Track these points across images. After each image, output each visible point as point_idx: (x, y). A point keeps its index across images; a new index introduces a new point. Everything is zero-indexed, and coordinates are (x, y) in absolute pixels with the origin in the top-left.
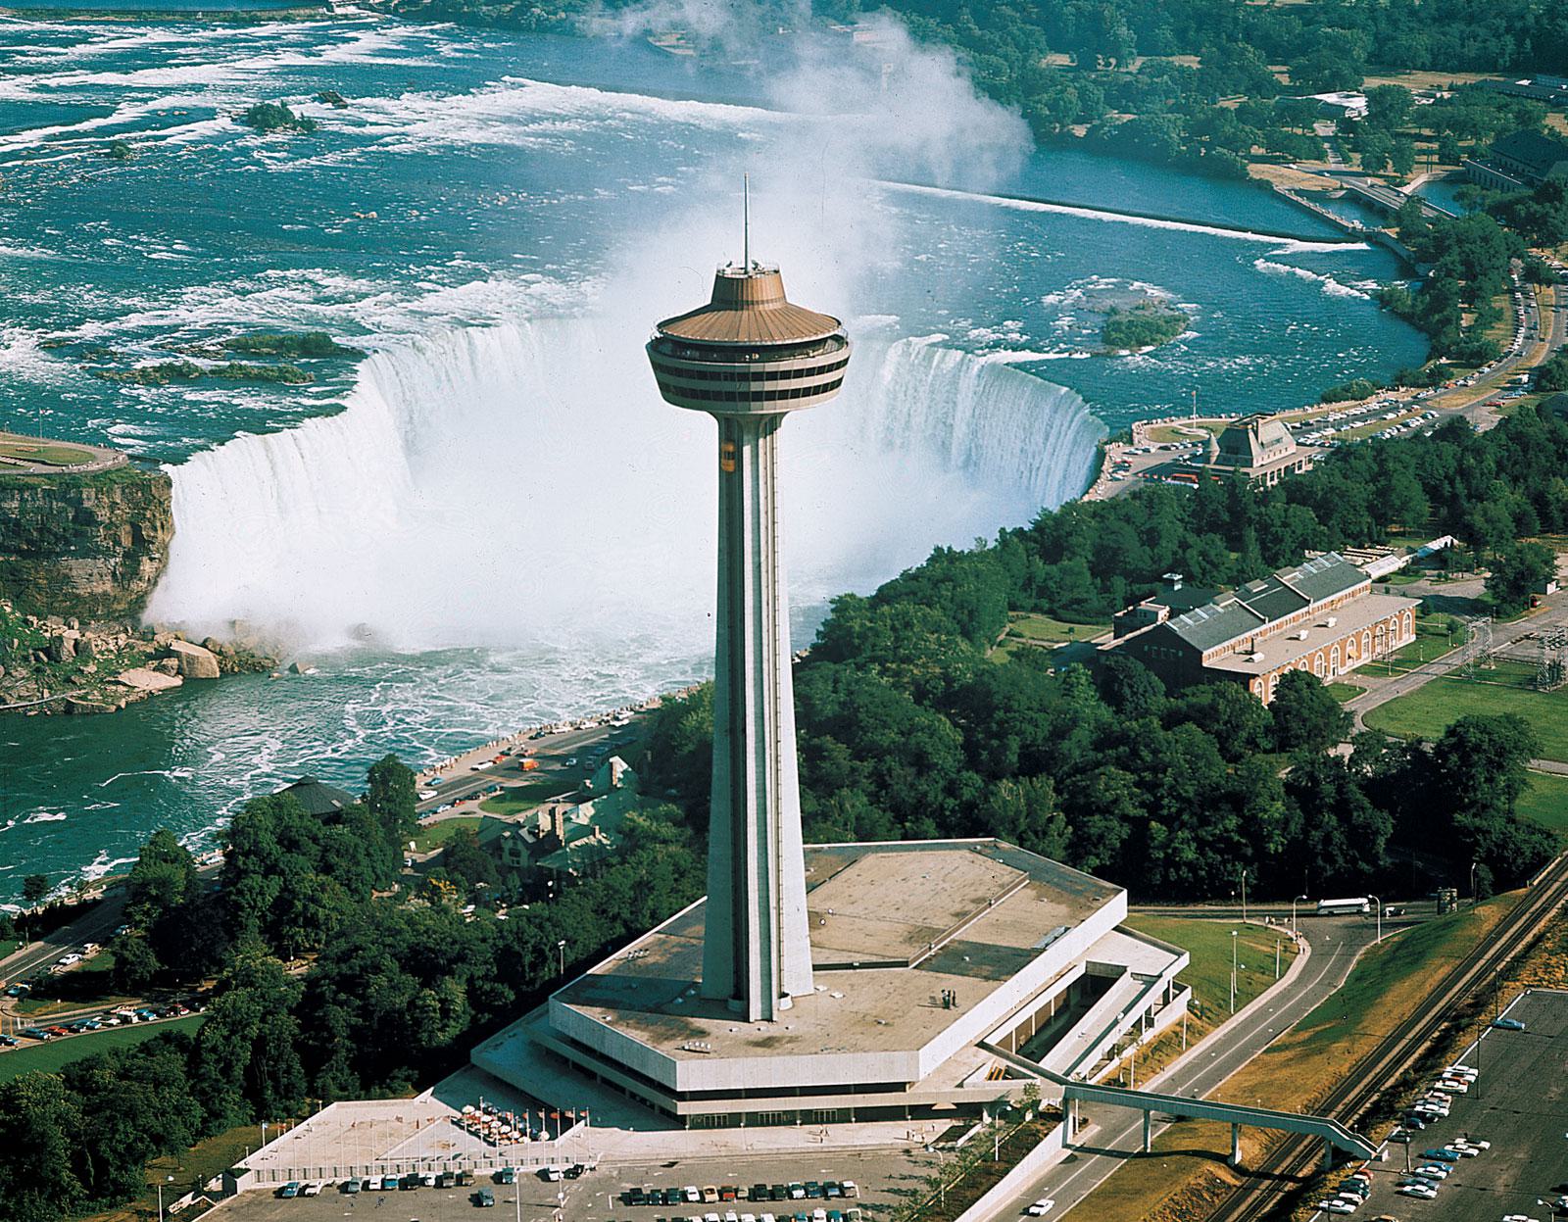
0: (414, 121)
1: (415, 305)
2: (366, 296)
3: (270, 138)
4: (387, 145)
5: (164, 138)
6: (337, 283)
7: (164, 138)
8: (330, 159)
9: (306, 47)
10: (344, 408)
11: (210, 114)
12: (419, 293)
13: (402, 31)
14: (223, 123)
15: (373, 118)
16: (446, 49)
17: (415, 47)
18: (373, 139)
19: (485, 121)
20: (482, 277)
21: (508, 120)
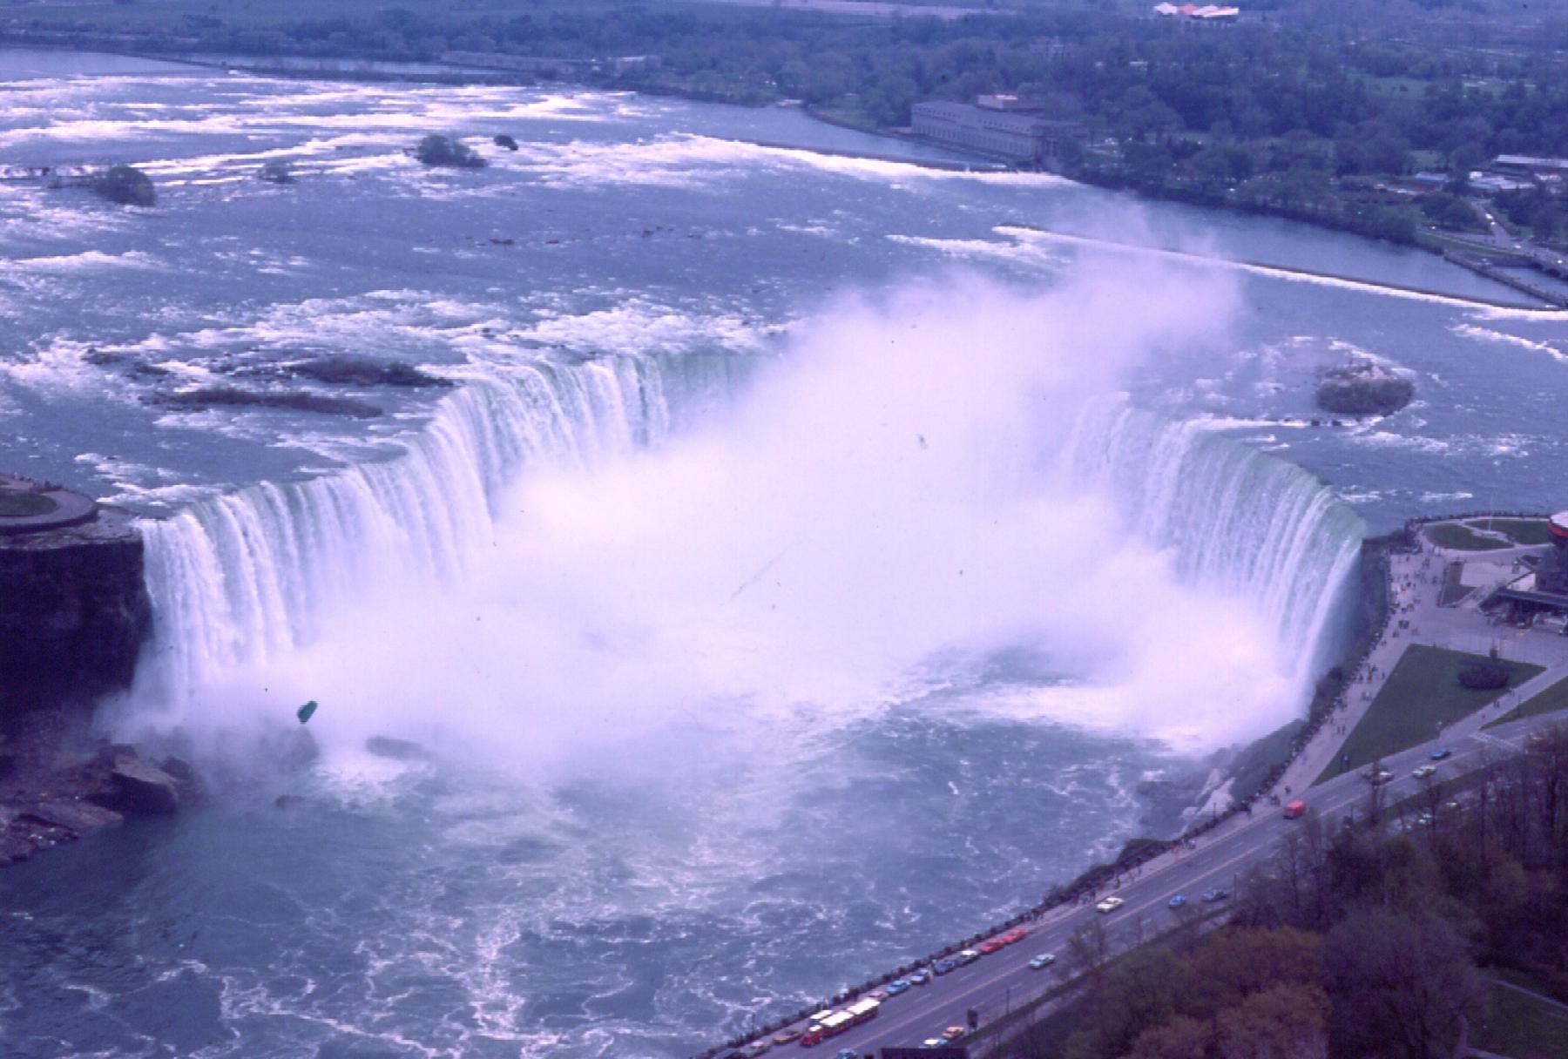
0: (577, 162)
1: (527, 334)
2: (467, 323)
3: (435, 171)
4: (545, 181)
5: (332, 167)
6: (446, 307)
7: (332, 167)
8: (487, 192)
9: (499, 106)
12: (534, 321)
14: (401, 159)
15: (540, 158)
16: (624, 110)
18: (534, 176)
19: (644, 167)
20: (605, 305)
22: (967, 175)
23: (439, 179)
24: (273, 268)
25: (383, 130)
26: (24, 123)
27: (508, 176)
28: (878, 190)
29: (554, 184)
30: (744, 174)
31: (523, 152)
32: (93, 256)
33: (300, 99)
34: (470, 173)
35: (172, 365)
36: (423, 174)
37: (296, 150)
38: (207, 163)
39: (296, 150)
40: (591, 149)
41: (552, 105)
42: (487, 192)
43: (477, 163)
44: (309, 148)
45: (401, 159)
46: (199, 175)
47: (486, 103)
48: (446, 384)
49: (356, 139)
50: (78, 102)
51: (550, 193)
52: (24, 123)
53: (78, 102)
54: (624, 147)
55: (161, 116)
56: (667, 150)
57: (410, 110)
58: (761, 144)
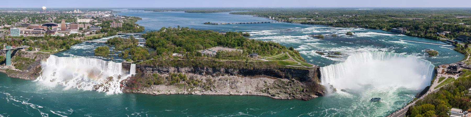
2: (351, 49)
3: (348, 35)
6: (349, 48)
8: (352, 37)
9: (353, 29)
10: (345, 62)
11: (343, 34)
13: (362, 28)
14: (344, 34)
16: (365, 30)
17: (363, 30)
21: (369, 35)
22: (396, 35)
23: (348, 36)
24: (333, 44)
25: (343, 32)
26: (311, 31)
27: (354, 36)
28: (388, 36)
29: (358, 37)
30: (376, 35)
31: (355, 34)
32: (317, 43)
33: (335, 29)
34: (351, 36)
35: (324, 53)
36: (346, 36)
37: (335, 34)
38: (327, 35)
39: (335, 34)
40: (362, 33)
41: (358, 29)
42: (352, 37)
43: (351, 35)
44: (337, 33)
45: (344, 34)
46: (326, 36)
47: (352, 29)
48: (349, 55)
49: (340, 33)
50: (316, 29)
51: (359, 38)
52: (311, 31)
53: (316, 29)
54: (365, 33)
55: (323, 30)
56: (369, 33)
57: (345, 30)
58: (377, 33)
